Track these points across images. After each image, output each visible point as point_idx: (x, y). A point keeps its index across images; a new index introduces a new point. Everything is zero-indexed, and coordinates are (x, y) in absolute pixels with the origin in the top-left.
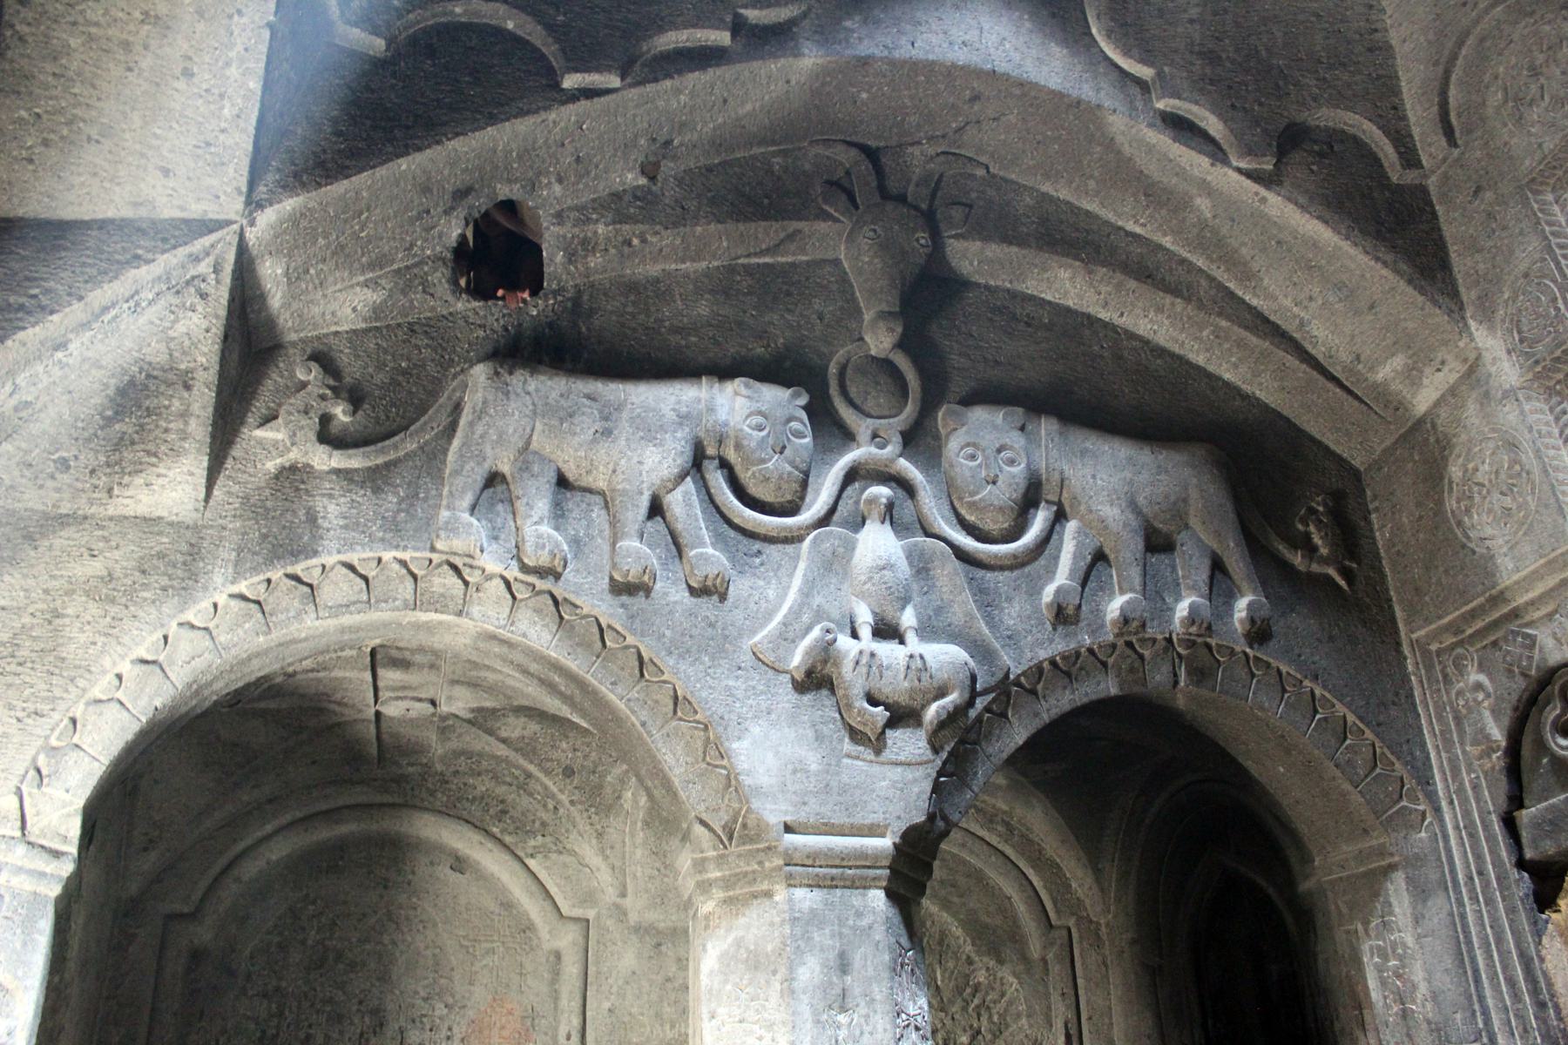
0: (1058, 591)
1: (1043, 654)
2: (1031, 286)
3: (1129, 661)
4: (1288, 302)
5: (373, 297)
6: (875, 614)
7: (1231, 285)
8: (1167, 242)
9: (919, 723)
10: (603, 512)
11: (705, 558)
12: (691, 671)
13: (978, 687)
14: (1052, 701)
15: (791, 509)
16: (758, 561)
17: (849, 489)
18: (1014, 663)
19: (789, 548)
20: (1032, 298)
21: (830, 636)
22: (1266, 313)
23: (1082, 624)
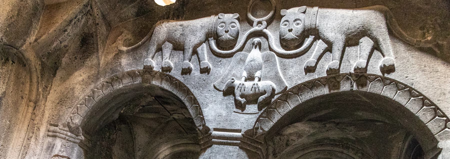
1: (300, 82)
9: (257, 103)
11: (204, 64)
13: (276, 93)
14: (303, 96)
16: (220, 63)
18: (289, 85)
19: (229, 59)
21: (232, 81)
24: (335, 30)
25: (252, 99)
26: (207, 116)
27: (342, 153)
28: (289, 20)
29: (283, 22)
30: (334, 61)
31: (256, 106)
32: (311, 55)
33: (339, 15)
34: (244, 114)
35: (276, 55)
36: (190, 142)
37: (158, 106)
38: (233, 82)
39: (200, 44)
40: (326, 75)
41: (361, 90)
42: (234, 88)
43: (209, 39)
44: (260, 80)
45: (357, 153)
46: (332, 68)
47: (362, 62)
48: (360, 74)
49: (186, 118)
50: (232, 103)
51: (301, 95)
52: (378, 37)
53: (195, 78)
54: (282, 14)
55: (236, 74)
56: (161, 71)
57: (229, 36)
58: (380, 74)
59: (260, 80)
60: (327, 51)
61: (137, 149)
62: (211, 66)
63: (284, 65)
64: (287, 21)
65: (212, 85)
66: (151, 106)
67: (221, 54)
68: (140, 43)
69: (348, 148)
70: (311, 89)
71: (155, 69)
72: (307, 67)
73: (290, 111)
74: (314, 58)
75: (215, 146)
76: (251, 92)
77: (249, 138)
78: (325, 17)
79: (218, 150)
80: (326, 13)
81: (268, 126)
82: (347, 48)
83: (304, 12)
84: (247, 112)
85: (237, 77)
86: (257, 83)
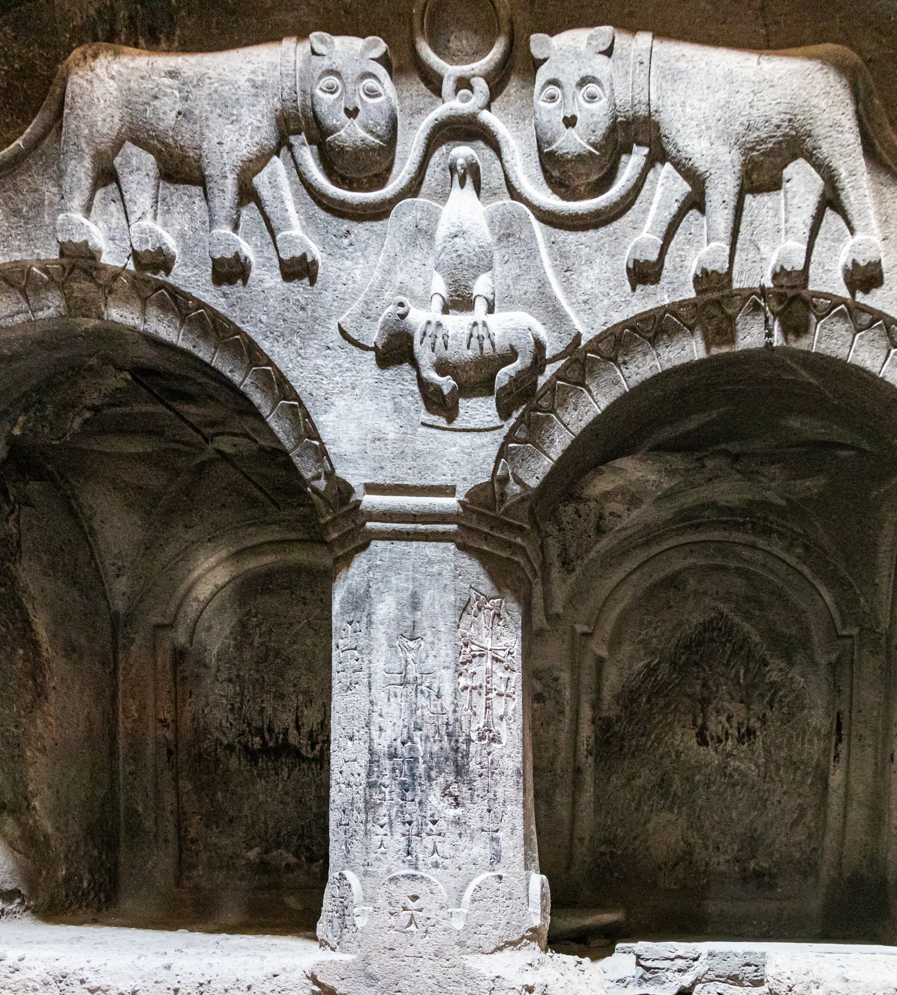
10: (203, 203)
11: (290, 241)
12: (284, 353)
15: (380, 180)
16: (346, 242)
17: (436, 157)
19: (377, 226)
24: (708, 128)
25: (476, 377)
27: (753, 547)
28: (562, 79)
30: (713, 244)
31: (492, 401)
32: (643, 221)
33: (719, 72)
34: (455, 430)
36: (293, 535)
37: (150, 408)
39: (260, 160)
41: (794, 345)
42: (410, 338)
43: (292, 139)
44: (491, 310)
45: (792, 545)
46: (710, 269)
47: (788, 250)
48: (791, 293)
49: (262, 449)
50: (412, 393)
51: (625, 363)
52: (834, 164)
54: (537, 52)
55: (410, 283)
56: (131, 266)
58: (843, 292)
59: (491, 310)
60: (691, 208)
61: (112, 570)
62: (316, 252)
63: (563, 255)
64: (554, 82)
66: (127, 410)
67: (343, 203)
68: (19, 142)
69: (767, 532)
70: (654, 341)
71: (105, 259)
72: (636, 262)
73: (597, 420)
74: (653, 233)
75: (378, 546)
76: (470, 353)
77: (484, 514)
78: (674, 76)
79: (391, 559)
80: (678, 60)
81: (536, 471)
82: (749, 198)
83: (608, 52)
84: (464, 425)
85: (413, 297)
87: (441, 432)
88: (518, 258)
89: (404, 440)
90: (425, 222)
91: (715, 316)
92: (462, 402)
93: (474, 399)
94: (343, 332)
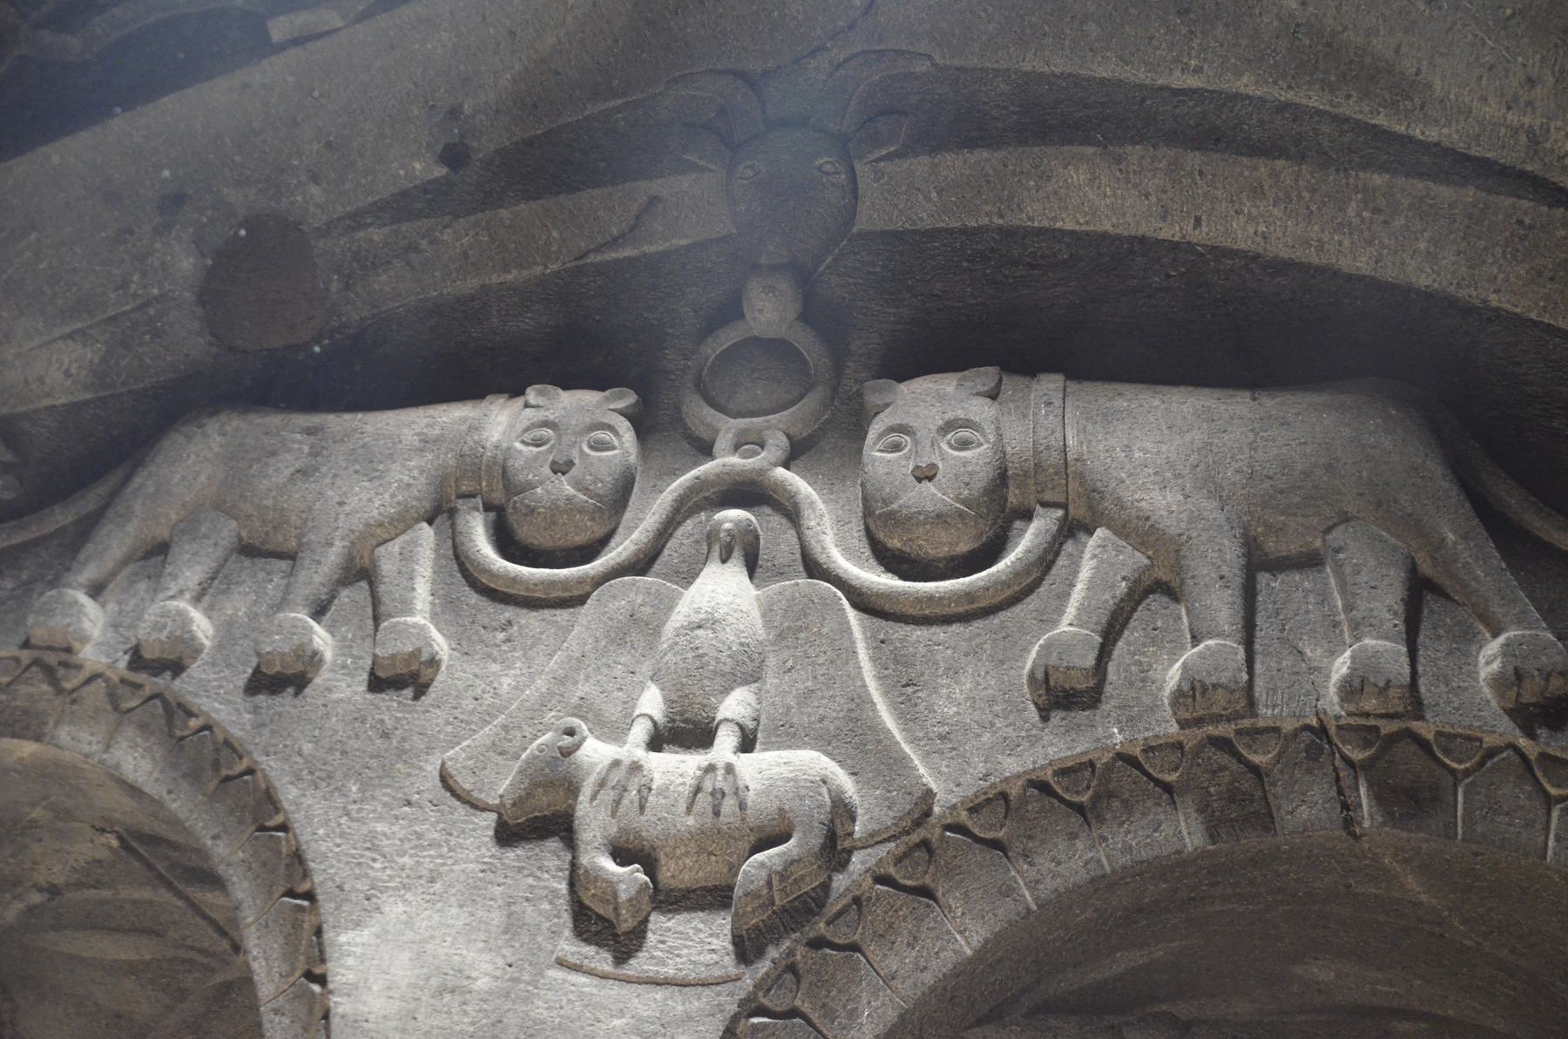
0: (1047, 648)
1: (1012, 766)
2: (1035, 212)
3: (1225, 777)
4: (1493, 110)
5: (90, 354)
6: (669, 701)
7: (1381, 120)
8: (1245, 84)
14: (1043, 863)
16: (501, 636)
17: (689, 525)
18: (944, 783)
19: (562, 615)
20: (1040, 232)
22: (1461, 147)
23: (1104, 707)
26: (352, 990)
29: (880, 436)
34: (628, 981)
35: (845, 602)
38: (567, 752)
39: (402, 523)
40: (1174, 728)
42: (572, 789)
53: (327, 716)
57: (569, 490)
59: (747, 744)
62: (441, 644)
65: (432, 768)
86: (731, 757)
87: (596, 981)
88: (813, 664)
89: (507, 995)
90: (648, 610)
91: (1222, 768)
92: (657, 921)
93: (685, 916)
94: (445, 780)
